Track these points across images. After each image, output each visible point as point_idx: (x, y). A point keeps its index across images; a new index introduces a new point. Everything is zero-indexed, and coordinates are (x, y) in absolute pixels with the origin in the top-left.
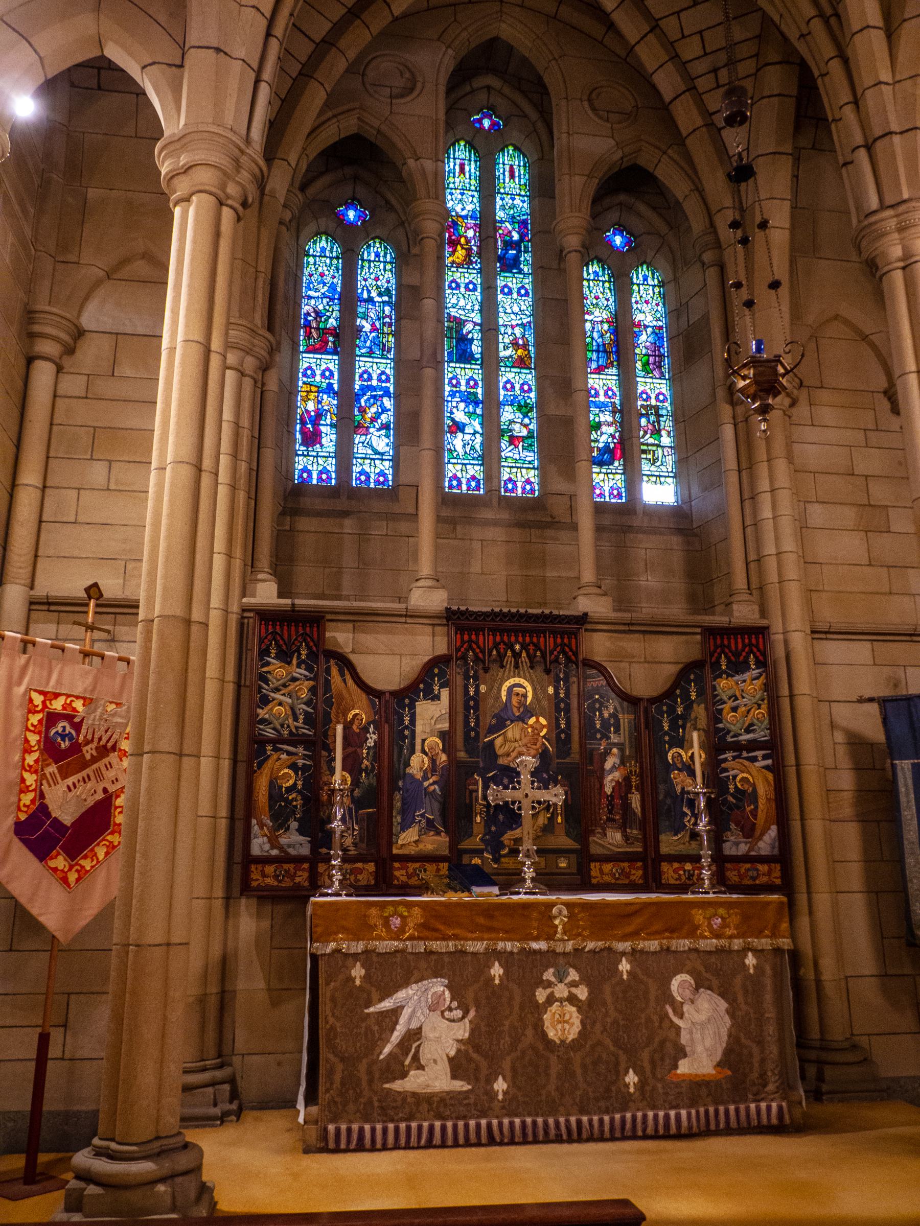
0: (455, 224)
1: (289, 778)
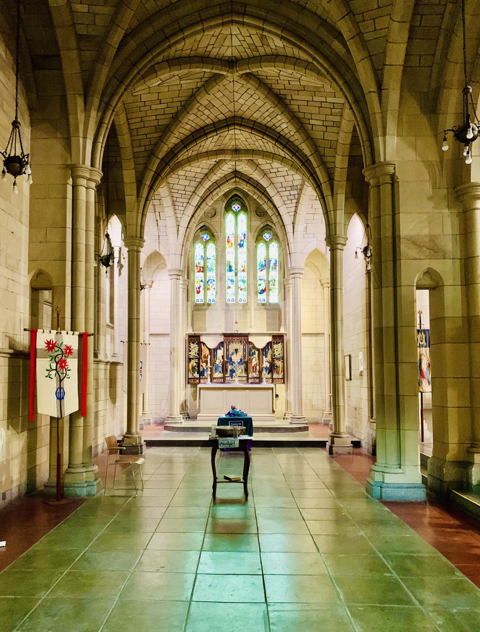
0: (228, 237)
1: (195, 364)
